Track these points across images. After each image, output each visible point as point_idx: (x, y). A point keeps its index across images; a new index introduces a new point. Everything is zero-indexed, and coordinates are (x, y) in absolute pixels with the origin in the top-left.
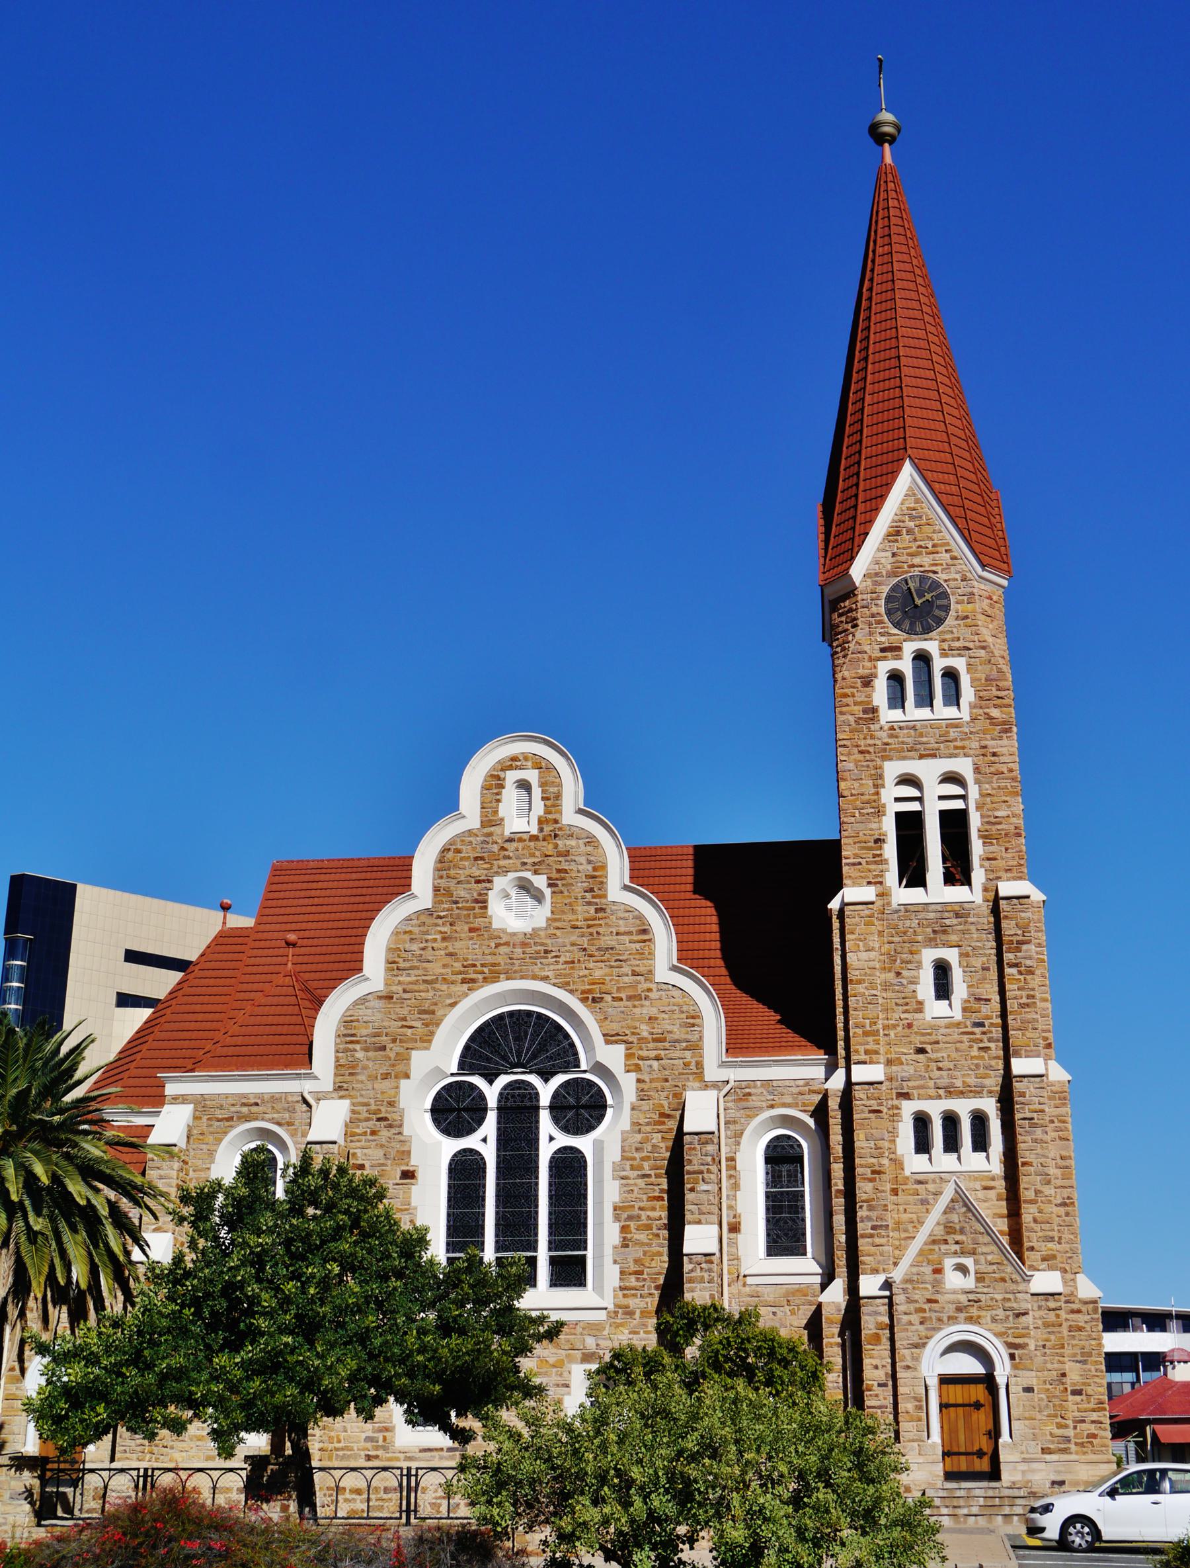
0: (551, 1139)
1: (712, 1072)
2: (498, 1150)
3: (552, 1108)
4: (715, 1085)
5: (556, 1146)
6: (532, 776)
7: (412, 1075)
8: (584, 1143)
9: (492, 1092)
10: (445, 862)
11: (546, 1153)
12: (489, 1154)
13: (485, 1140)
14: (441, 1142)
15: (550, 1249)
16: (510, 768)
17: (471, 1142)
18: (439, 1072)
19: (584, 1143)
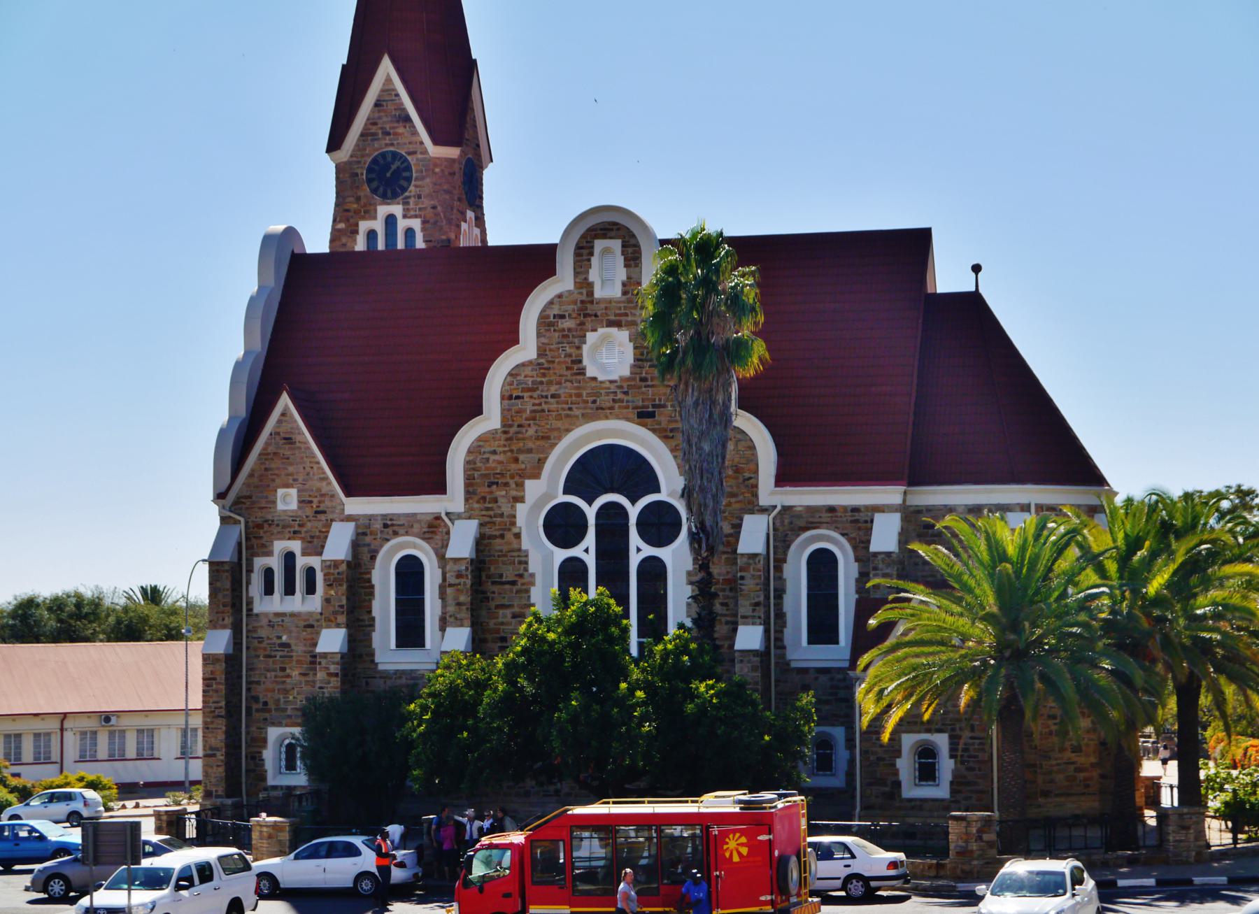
0: (639, 550)
1: (764, 499)
2: (597, 559)
3: (638, 524)
4: (764, 510)
5: (642, 555)
6: (616, 245)
7: (527, 498)
8: (664, 553)
9: (591, 512)
10: (546, 323)
11: (635, 560)
12: (591, 561)
13: (586, 551)
14: (552, 553)
15: (639, 637)
16: (597, 237)
17: (576, 552)
18: (547, 496)
19: (664, 553)
